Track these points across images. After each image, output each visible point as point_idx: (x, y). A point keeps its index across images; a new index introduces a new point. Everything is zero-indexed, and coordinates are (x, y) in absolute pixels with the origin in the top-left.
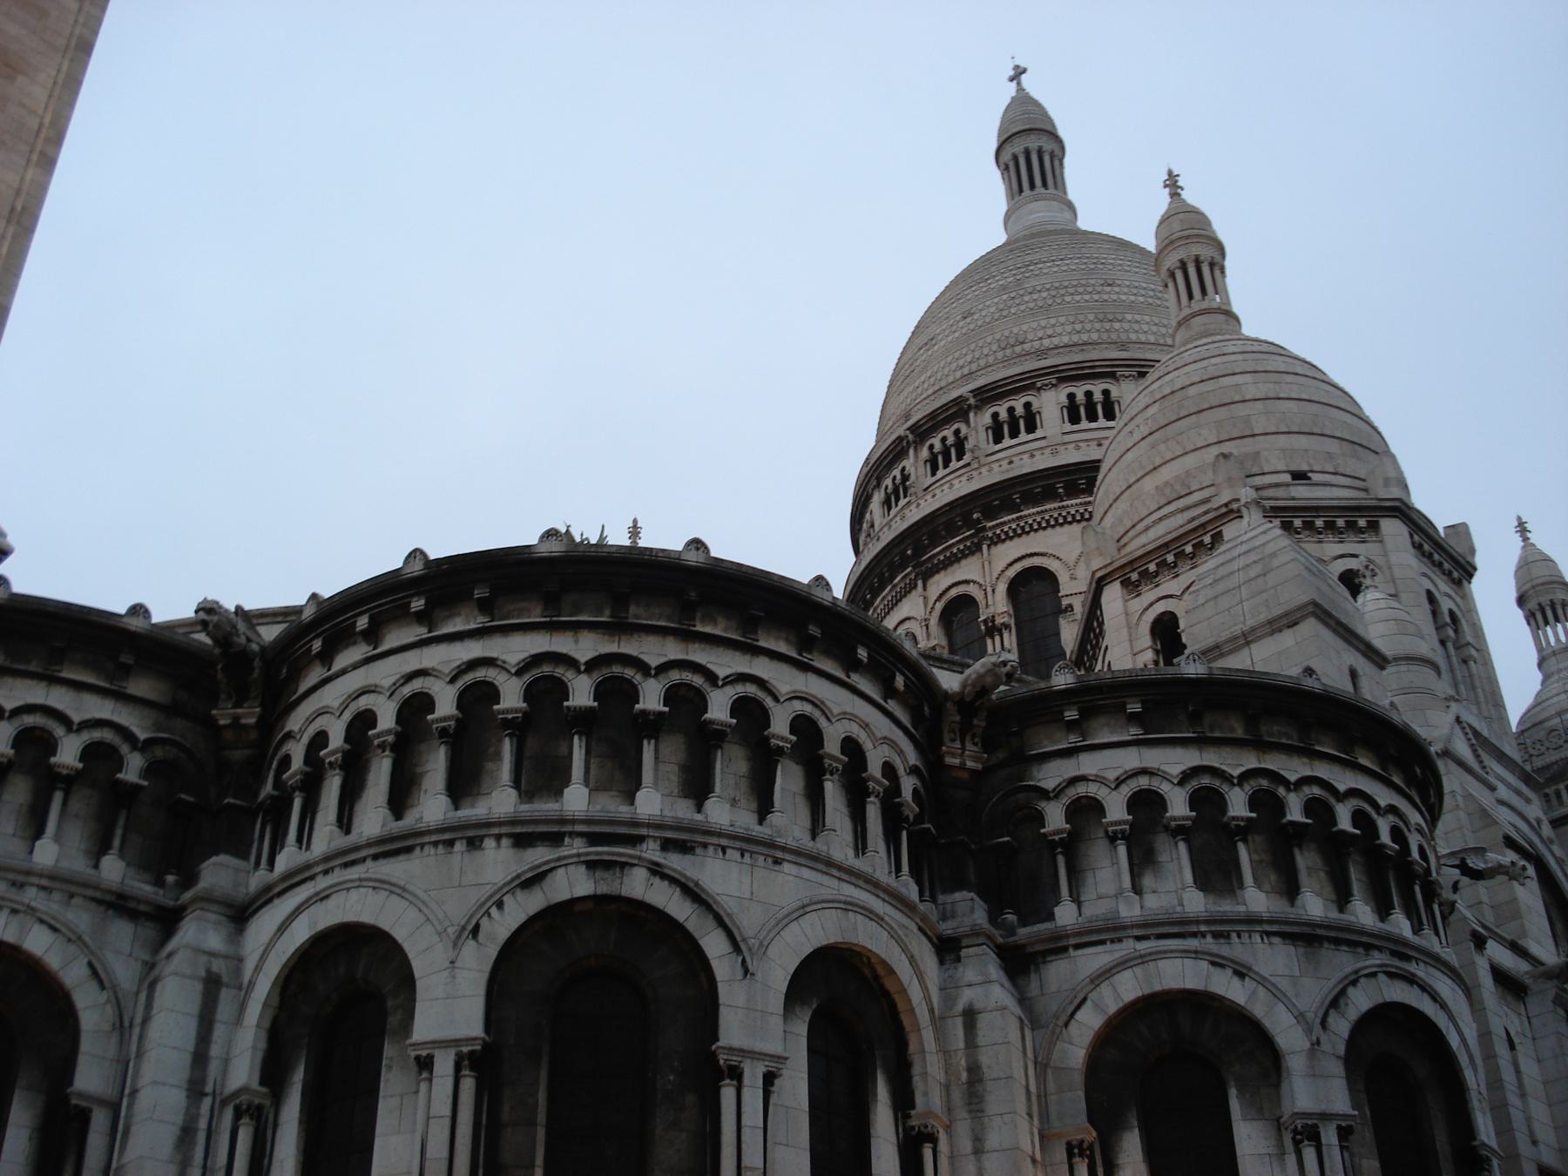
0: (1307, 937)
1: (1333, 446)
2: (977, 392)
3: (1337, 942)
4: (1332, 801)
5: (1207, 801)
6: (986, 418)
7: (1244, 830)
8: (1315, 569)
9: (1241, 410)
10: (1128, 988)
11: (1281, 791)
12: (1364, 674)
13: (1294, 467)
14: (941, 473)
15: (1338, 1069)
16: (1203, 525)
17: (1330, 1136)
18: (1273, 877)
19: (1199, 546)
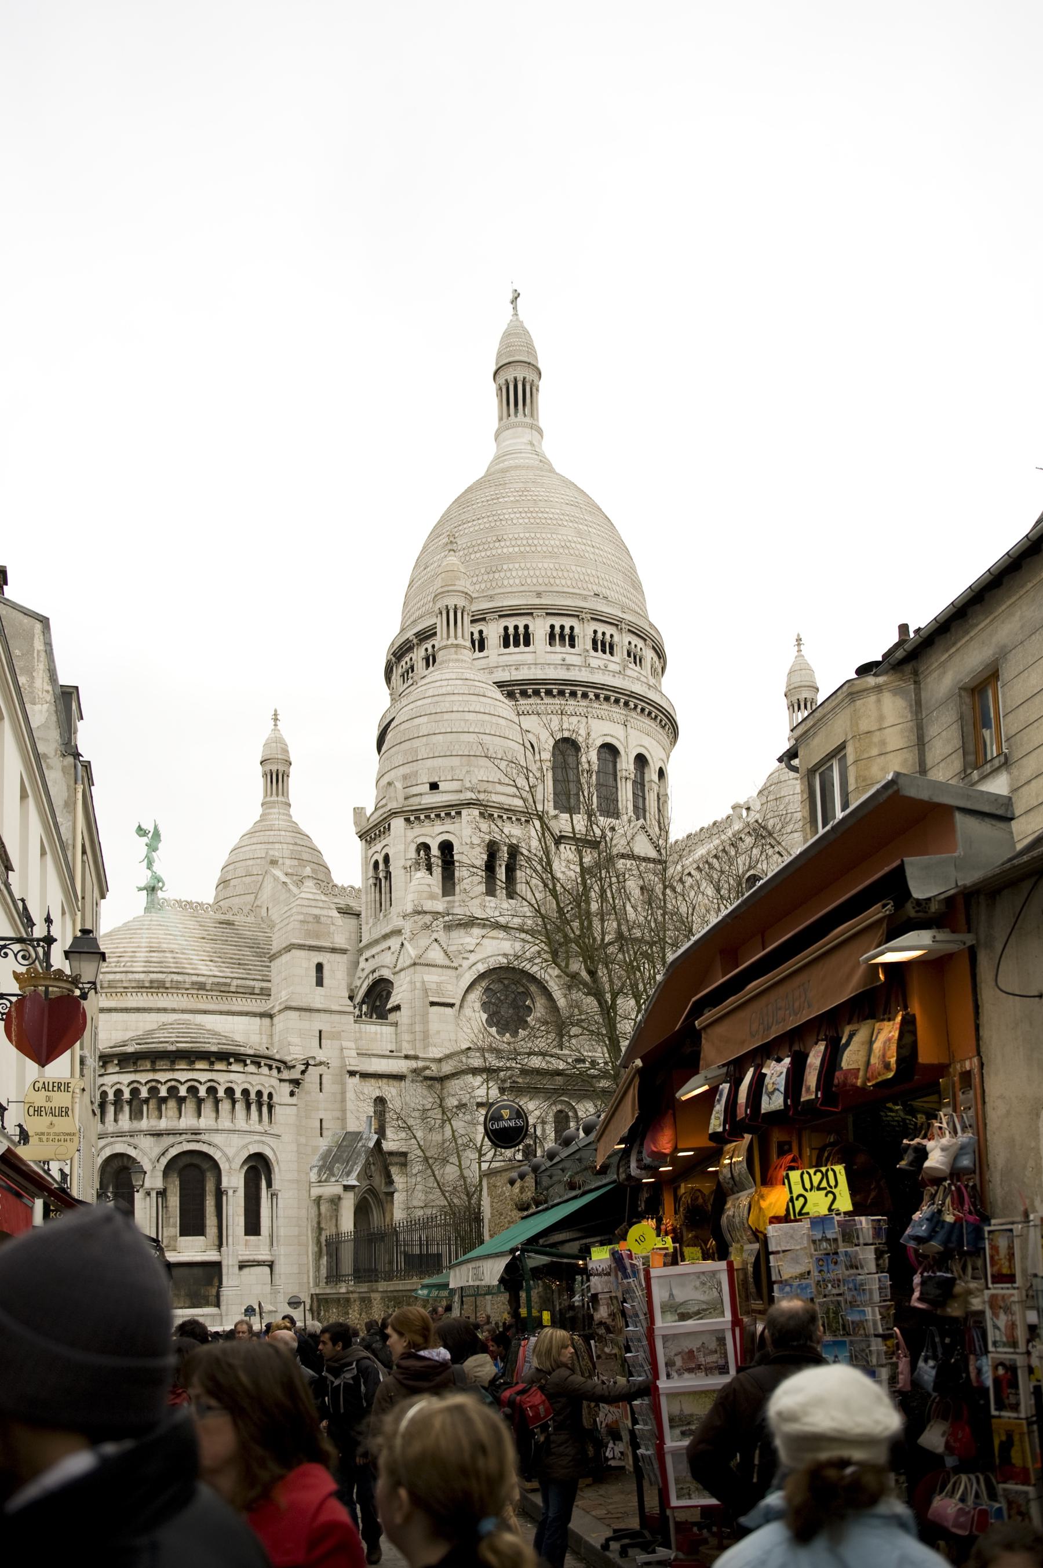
0: (158, 1134)
1: (456, 761)
2: (417, 635)
3: (169, 1134)
4: (179, 1085)
5: (135, 1092)
6: (422, 653)
7: (146, 1101)
8: (311, 919)
9: (416, 743)
10: (107, 1152)
11: (159, 1086)
12: (329, 962)
13: (432, 780)
14: (406, 685)
15: (161, 1174)
16: (385, 818)
17: (154, 1194)
18: (157, 1113)
19: (384, 828)
